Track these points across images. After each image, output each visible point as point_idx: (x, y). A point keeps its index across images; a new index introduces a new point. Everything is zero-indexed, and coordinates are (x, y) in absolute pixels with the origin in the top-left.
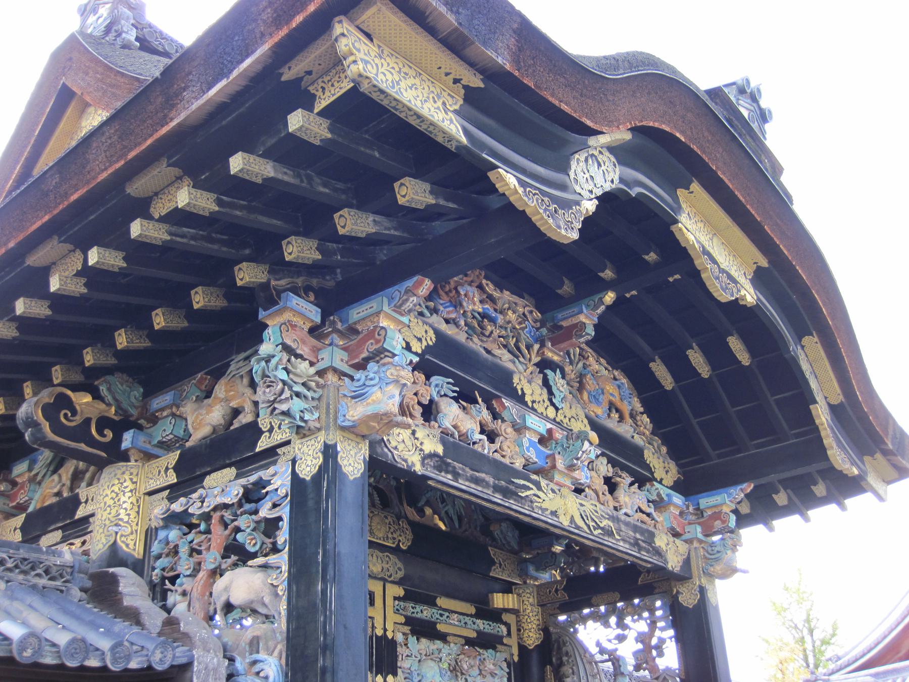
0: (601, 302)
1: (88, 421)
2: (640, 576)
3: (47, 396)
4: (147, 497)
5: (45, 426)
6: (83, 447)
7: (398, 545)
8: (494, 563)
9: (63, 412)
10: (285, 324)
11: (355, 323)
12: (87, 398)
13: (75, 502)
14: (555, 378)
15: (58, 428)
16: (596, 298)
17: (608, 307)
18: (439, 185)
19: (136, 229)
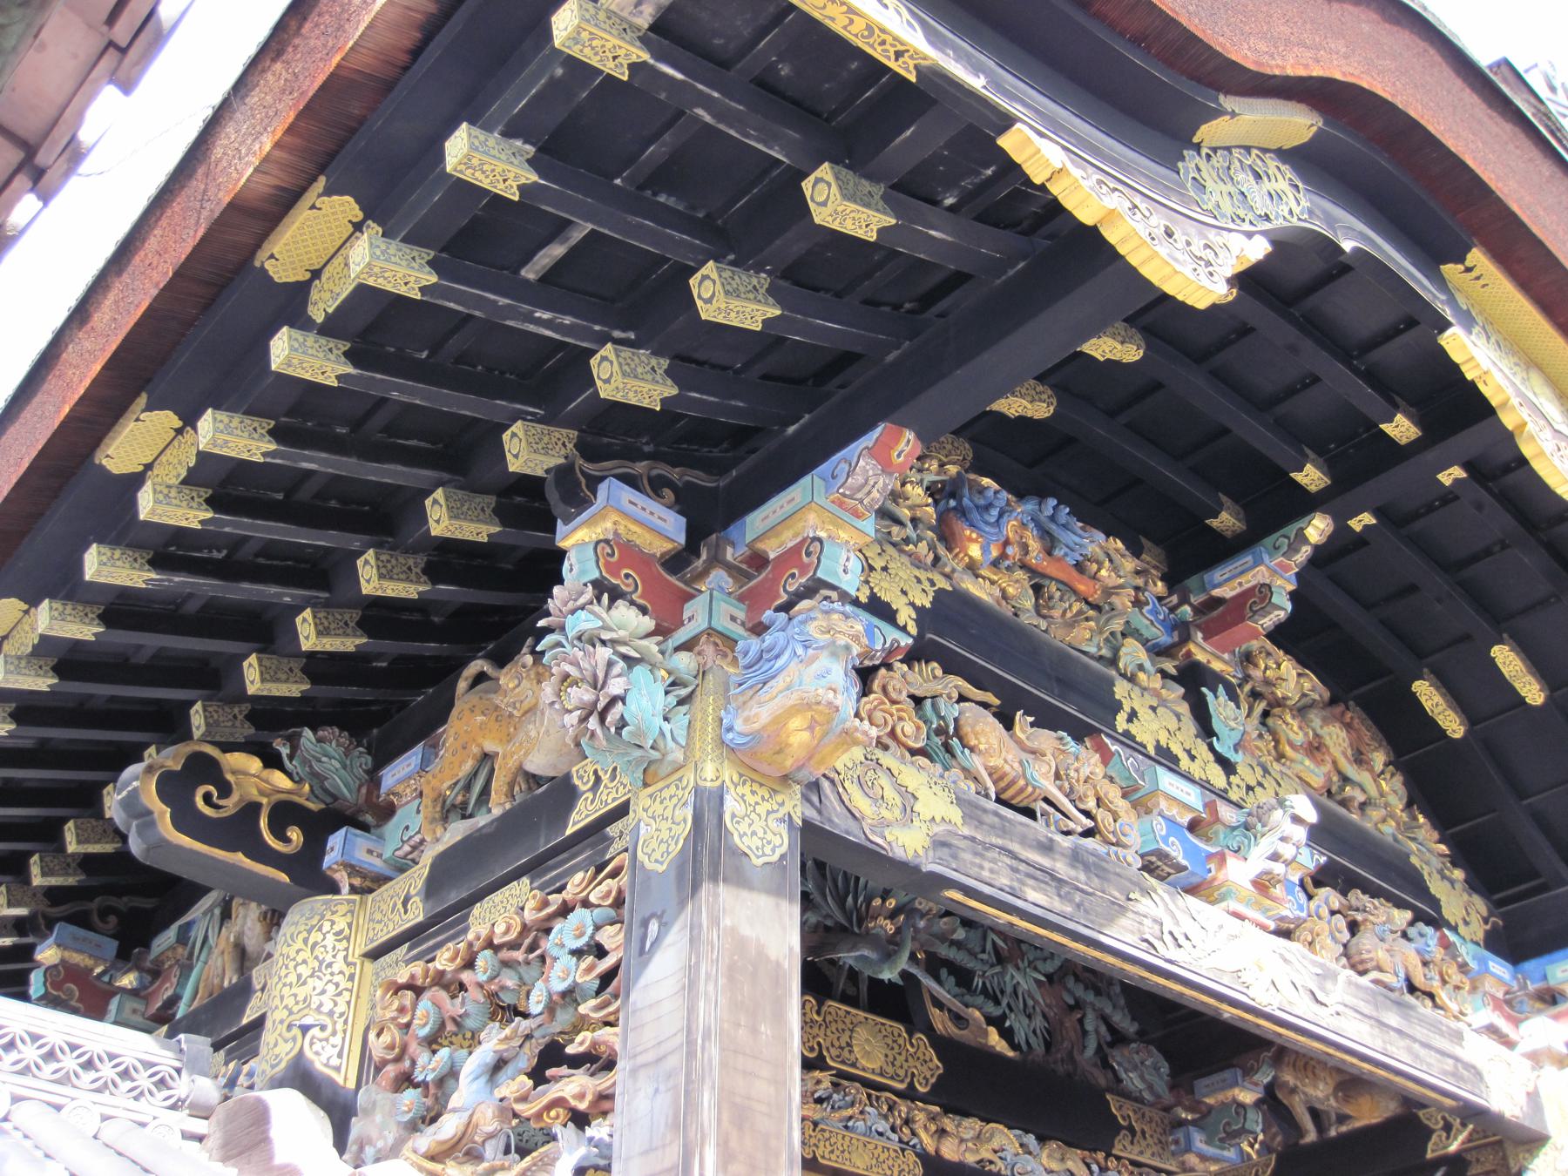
0: (1302, 538)
1: (252, 809)
2: (1429, 1138)
3: (172, 758)
4: (369, 965)
5: (163, 813)
6: (239, 858)
7: (911, 1085)
8: (1119, 1128)
9: (201, 791)
10: (607, 541)
11: (761, 538)
12: (254, 764)
13: (243, 991)
14: (1220, 706)
15: (186, 819)
16: (1291, 530)
17: (1317, 548)
18: (910, 190)
19: (287, 352)
